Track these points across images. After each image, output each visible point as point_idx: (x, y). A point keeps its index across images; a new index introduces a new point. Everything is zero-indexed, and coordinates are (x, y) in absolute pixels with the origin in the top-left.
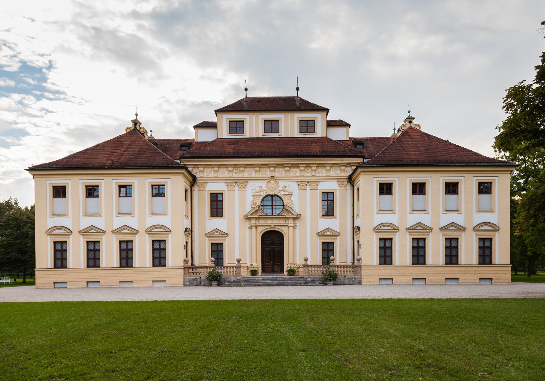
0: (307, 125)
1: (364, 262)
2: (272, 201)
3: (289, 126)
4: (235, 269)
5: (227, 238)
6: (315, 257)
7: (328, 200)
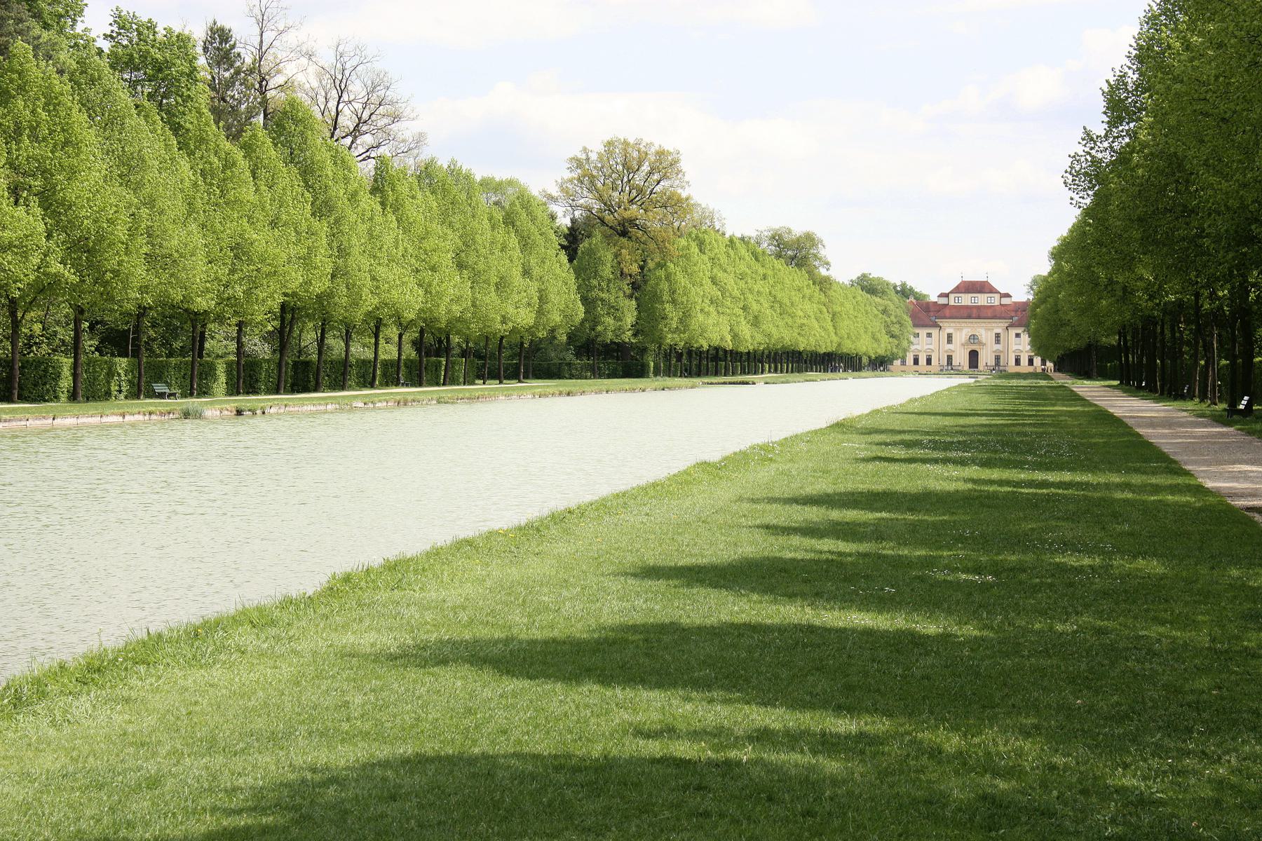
2: (973, 338)
3: (982, 300)
6: (992, 362)
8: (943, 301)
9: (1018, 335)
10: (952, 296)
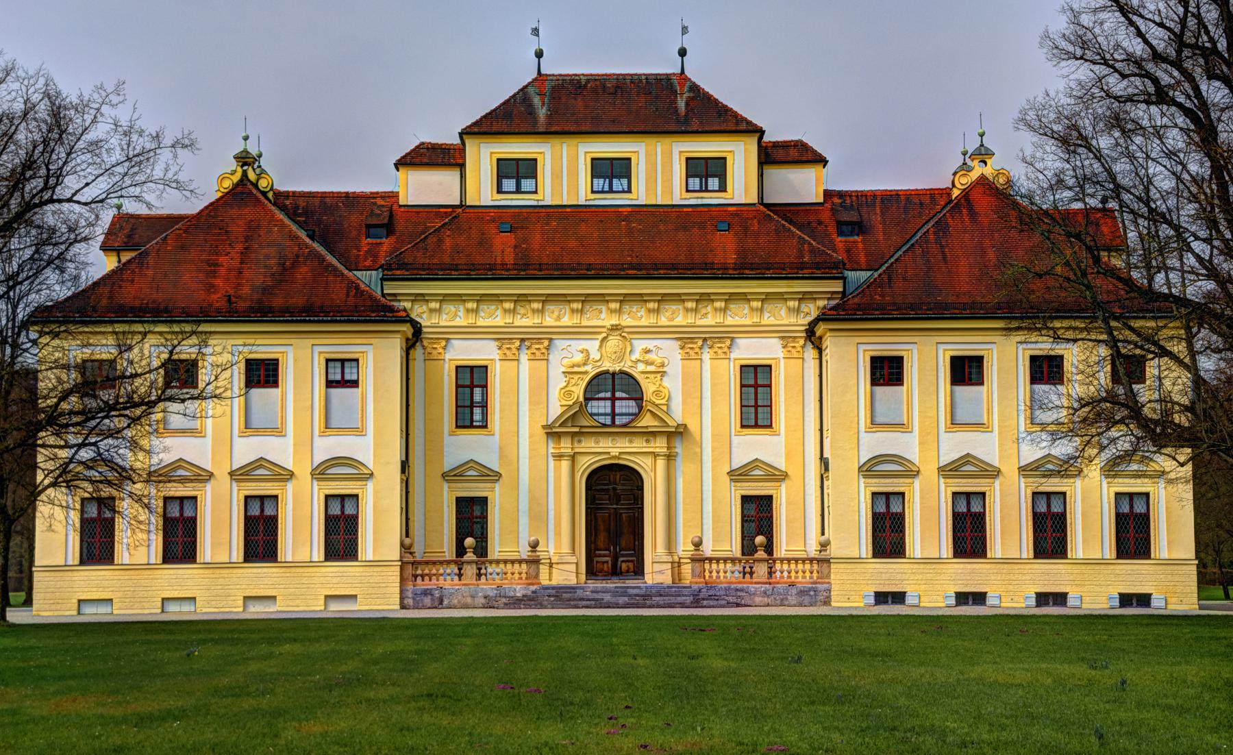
0: (706, 170)
1: (834, 551)
2: (614, 393)
3: (658, 172)
4: (524, 566)
5: (497, 485)
6: (722, 535)
7: (756, 386)
8: (428, 188)
9: (887, 371)
10: (483, 157)
